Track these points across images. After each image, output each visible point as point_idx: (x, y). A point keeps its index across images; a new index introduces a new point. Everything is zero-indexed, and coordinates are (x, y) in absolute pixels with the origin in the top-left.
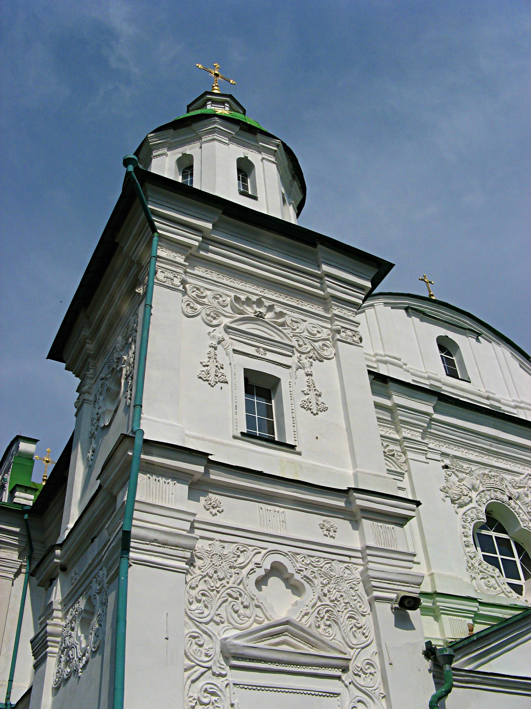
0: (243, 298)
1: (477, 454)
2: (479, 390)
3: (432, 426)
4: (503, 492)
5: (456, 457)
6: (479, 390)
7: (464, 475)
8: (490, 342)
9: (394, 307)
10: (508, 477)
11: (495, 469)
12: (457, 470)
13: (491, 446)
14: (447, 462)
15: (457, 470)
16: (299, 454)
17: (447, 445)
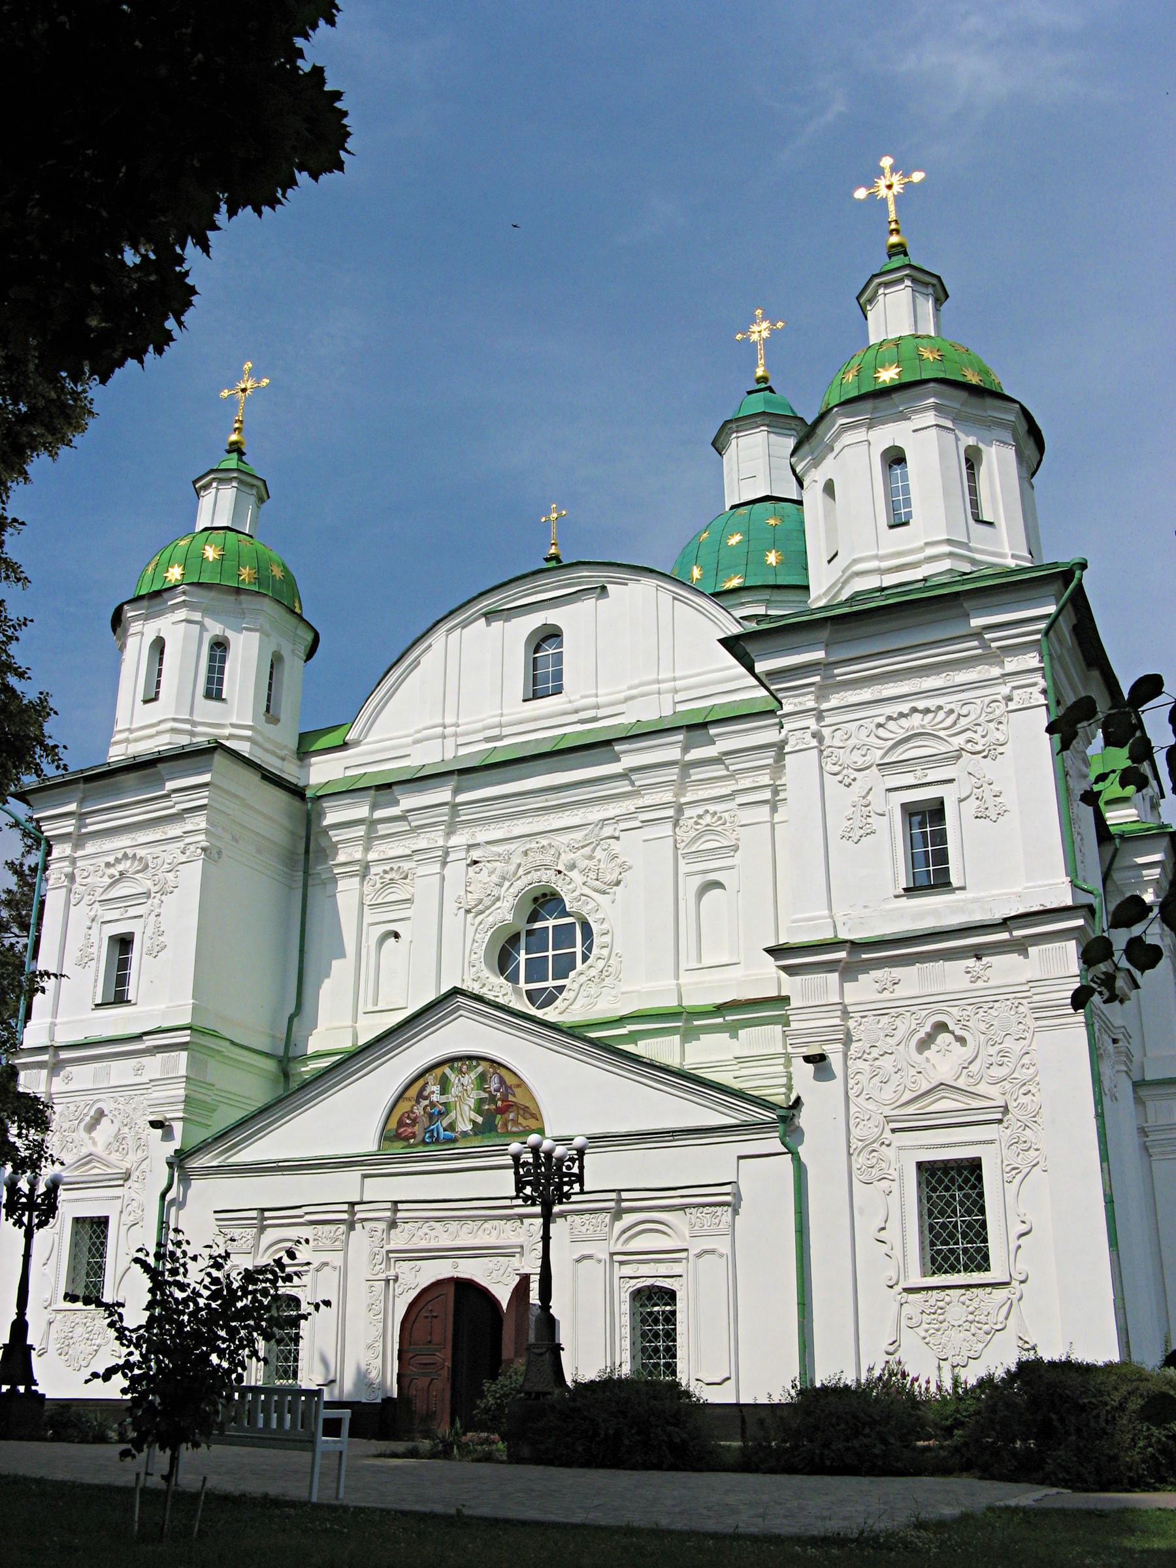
0: (111, 859)
1: (530, 819)
2: (570, 702)
3: (461, 812)
4: (547, 867)
5: (488, 843)
6: (570, 702)
7: (498, 863)
8: (626, 584)
9: (465, 624)
10: (565, 838)
11: (548, 834)
12: (488, 861)
13: (547, 801)
14: (475, 854)
15: (488, 861)
16: (135, 1004)
17: (487, 827)
